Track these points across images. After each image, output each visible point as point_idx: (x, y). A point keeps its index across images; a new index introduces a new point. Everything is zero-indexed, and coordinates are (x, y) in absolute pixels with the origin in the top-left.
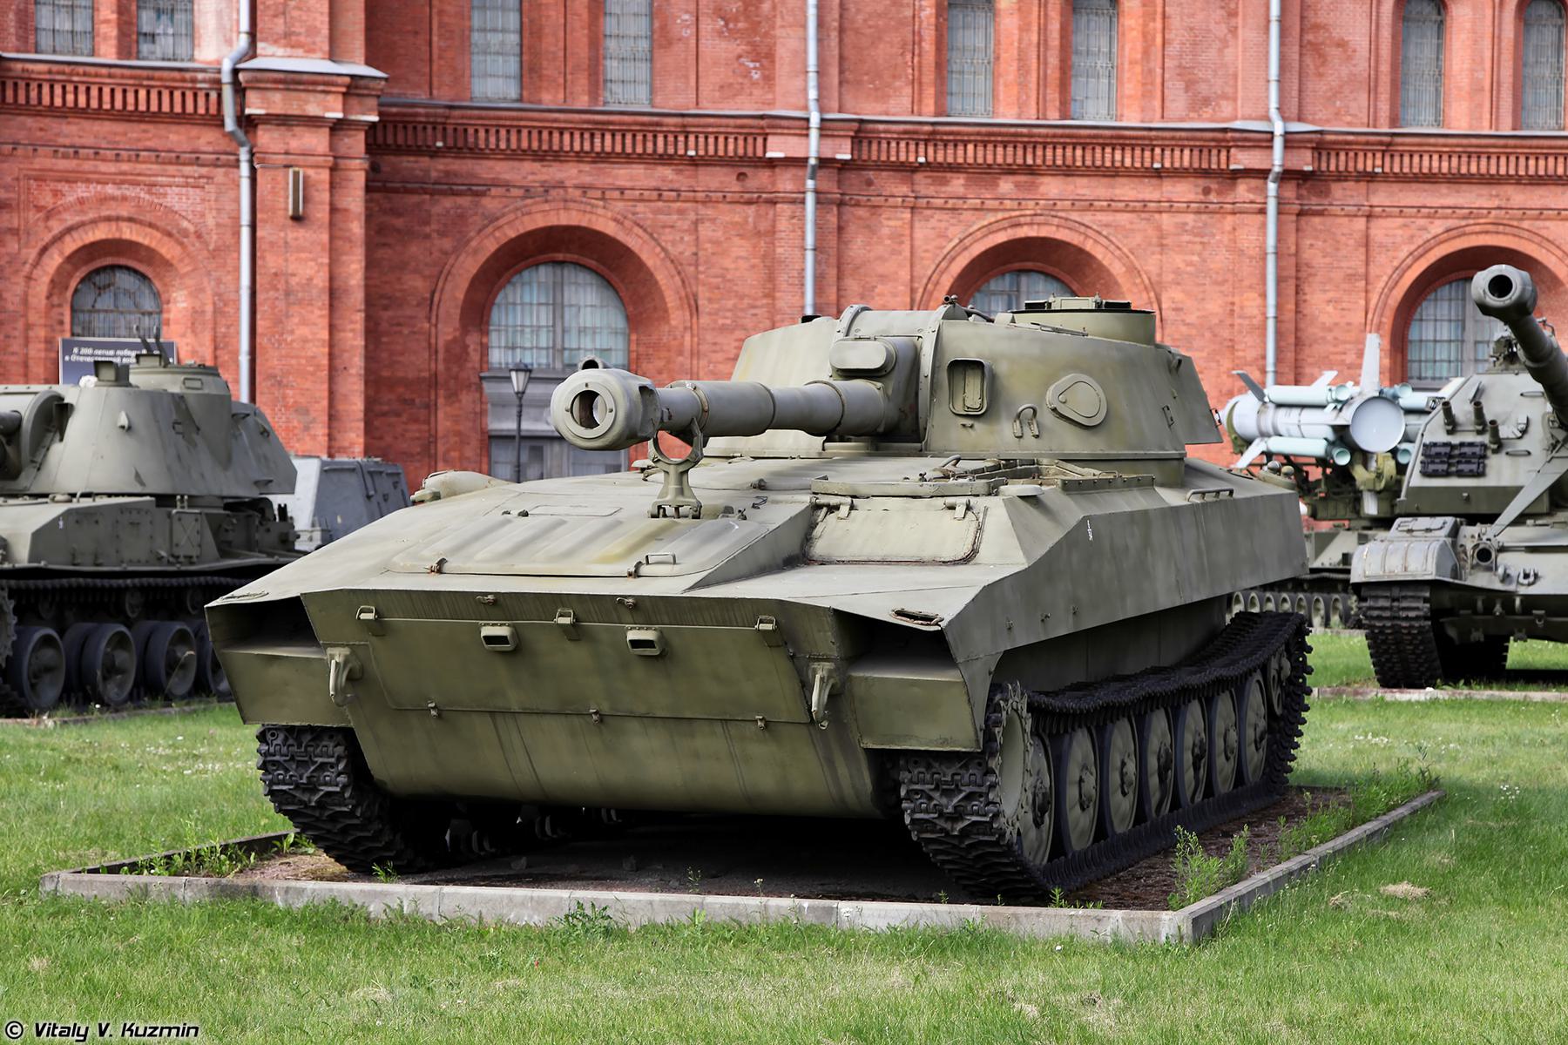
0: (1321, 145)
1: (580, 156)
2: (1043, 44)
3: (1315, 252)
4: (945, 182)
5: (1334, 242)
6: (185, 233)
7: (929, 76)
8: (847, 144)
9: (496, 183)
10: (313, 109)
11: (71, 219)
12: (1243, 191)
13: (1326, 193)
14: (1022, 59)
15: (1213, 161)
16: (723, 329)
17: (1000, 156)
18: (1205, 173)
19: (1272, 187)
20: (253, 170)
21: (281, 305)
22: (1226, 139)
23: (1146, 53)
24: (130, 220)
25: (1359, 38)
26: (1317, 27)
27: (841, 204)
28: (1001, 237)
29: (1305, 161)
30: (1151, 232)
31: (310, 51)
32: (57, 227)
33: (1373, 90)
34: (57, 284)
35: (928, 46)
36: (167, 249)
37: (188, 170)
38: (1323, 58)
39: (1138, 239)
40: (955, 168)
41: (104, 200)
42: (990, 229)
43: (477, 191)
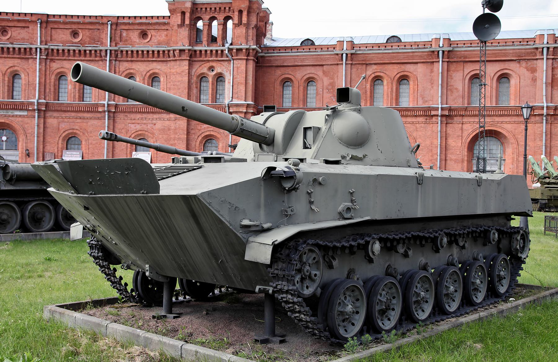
0: (450, 109)
2: (392, 91)
3: (450, 130)
5: (454, 129)
7: (368, 99)
10: (241, 110)
11: (203, 131)
12: (434, 119)
13: (453, 119)
15: (427, 113)
18: (426, 116)
19: (439, 118)
22: (430, 109)
23: (414, 92)
25: (460, 88)
26: (451, 86)
30: (415, 128)
31: (241, 100)
32: (201, 132)
33: (463, 98)
34: (201, 142)
35: (368, 93)
38: (452, 92)
39: (411, 129)
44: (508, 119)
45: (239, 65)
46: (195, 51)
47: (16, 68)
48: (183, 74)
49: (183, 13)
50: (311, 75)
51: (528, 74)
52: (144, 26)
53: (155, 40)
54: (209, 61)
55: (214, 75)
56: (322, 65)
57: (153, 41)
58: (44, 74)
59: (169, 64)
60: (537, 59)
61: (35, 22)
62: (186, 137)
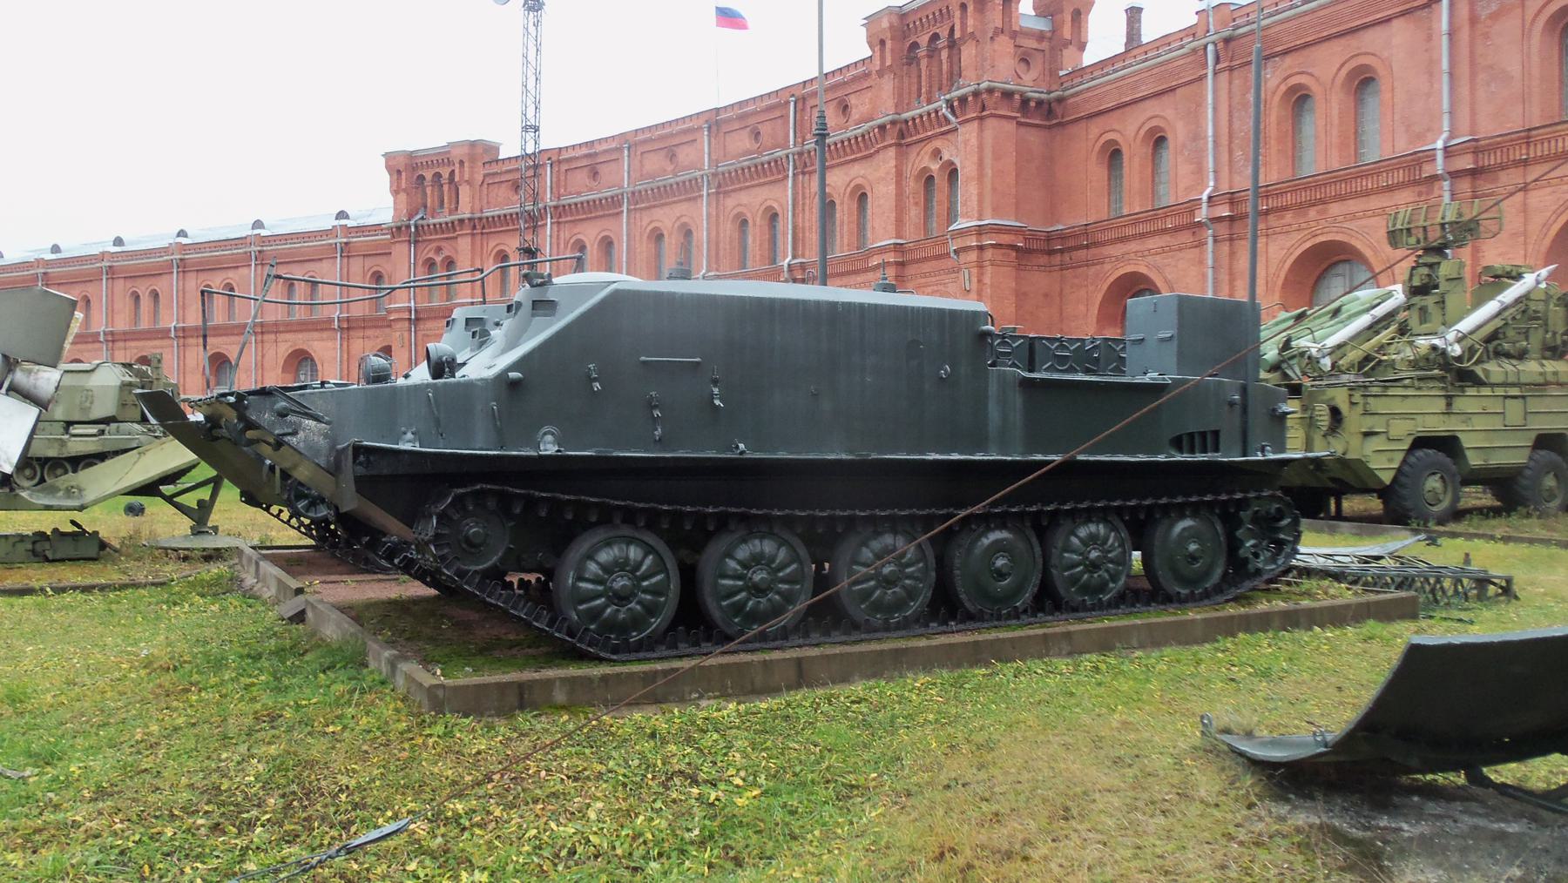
0: (1476, 148)
1: (1134, 237)
4: (1282, 217)
8: (1227, 207)
13: (1495, 180)
17: (1304, 196)
18: (1416, 183)
19: (1446, 184)
25: (1515, 69)
27: (1231, 240)
28: (1308, 245)
29: (1466, 162)
40: (1285, 209)
43: (1100, 261)
46: (906, 122)
47: (684, 219)
49: (882, 42)
50: (1154, 123)
52: (841, 87)
53: (855, 115)
54: (929, 138)
56: (1172, 90)
58: (714, 220)
61: (700, 128)
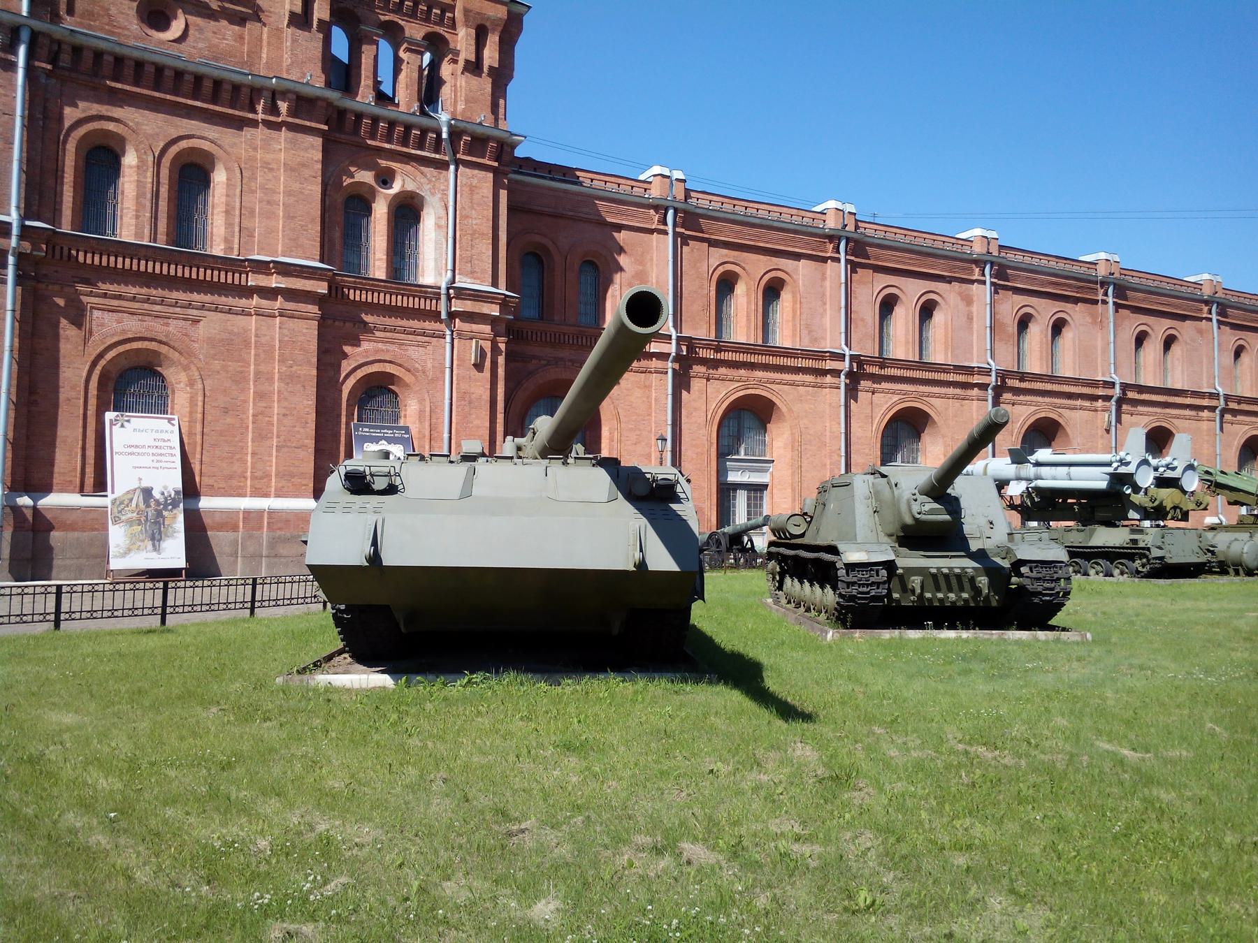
6: (417, 371)
9: (534, 357)
12: (829, 379)
14: (748, 316)
16: (631, 430)
19: (843, 377)
20: (453, 339)
21: (467, 409)
23: (794, 317)
24: (390, 362)
31: (482, 282)
36: (407, 378)
37: (419, 338)
41: (377, 351)
42: (737, 390)
44: (936, 390)
45: (475, 182)
48: (307, 173)
51: (962, 306)
55: (396, 196)
57: (190, 39)
59: (248, 132)
60: (972, 282)
62: (315, 372)
